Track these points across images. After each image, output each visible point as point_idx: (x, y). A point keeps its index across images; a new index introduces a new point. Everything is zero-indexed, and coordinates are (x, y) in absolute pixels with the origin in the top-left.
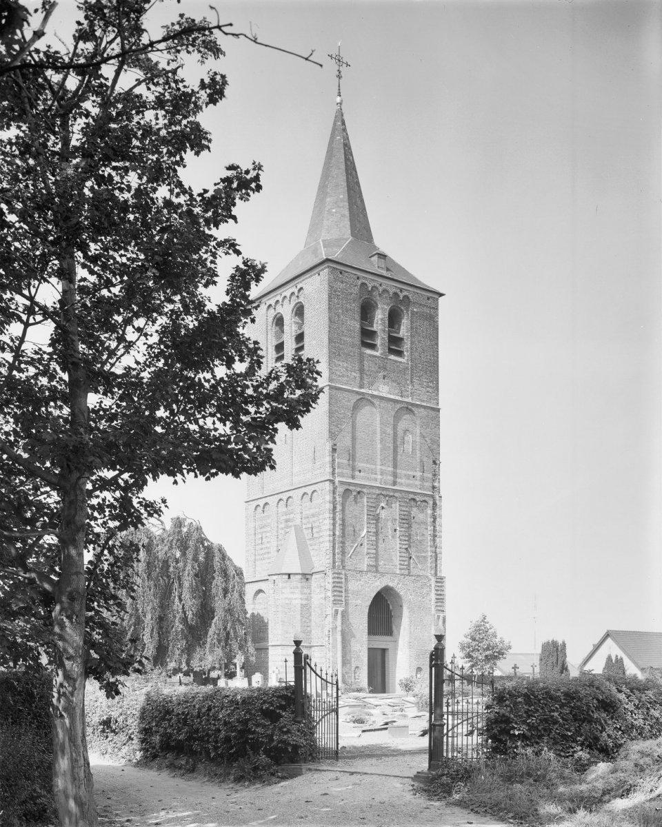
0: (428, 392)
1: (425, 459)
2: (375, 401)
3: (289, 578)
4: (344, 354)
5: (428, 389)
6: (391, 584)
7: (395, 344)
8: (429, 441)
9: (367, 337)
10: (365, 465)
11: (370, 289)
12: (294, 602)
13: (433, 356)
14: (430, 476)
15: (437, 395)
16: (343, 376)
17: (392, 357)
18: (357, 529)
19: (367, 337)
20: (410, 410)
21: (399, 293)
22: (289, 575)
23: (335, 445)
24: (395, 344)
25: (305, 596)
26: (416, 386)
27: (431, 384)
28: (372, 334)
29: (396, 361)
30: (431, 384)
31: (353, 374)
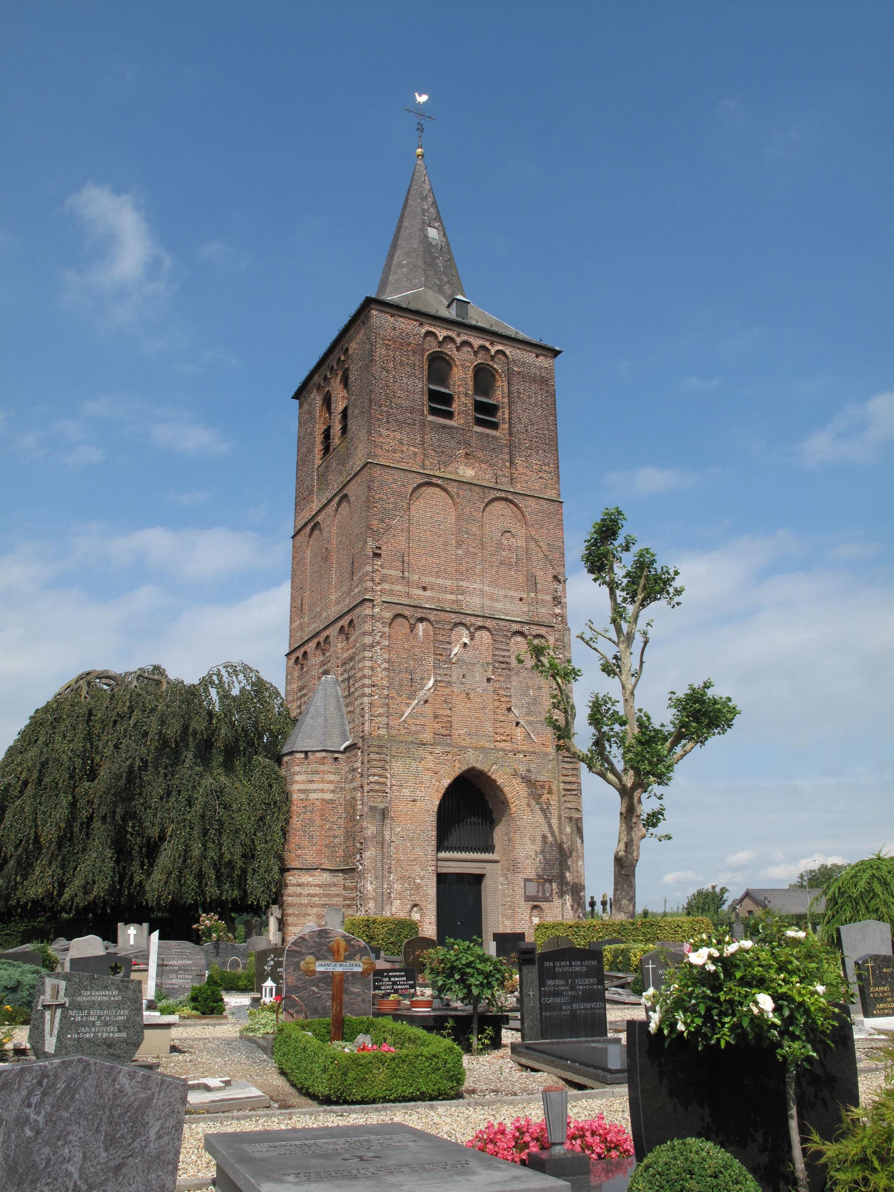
0: (540, 478)
1: (540, 574)
2: (453, 488)
3: (306, 757)
4: (396, 421)
5: (541, 474)
6: (478, 766)
7: (486, 413)
8: (545, 547)
9: (440, 402)
10: (433, 580)
11: (441, 339)
12: (313, 796)
13: (549, 430)
14: (549, 598)
15: (558, 482)
16: (394, 451)
17: (477, 429)
18: (417, 677)
19: (440, 402)
20: (511, 502)
21: (490, 347)
22: (306, 753)
23: (380, 548)
24: (486, 413)
25: (331, 787)
26: (520, 470)
27: (547, 468)
28: (447, 399)
29: (488, 435)
30: (547, 468)
31: (412, 448)
